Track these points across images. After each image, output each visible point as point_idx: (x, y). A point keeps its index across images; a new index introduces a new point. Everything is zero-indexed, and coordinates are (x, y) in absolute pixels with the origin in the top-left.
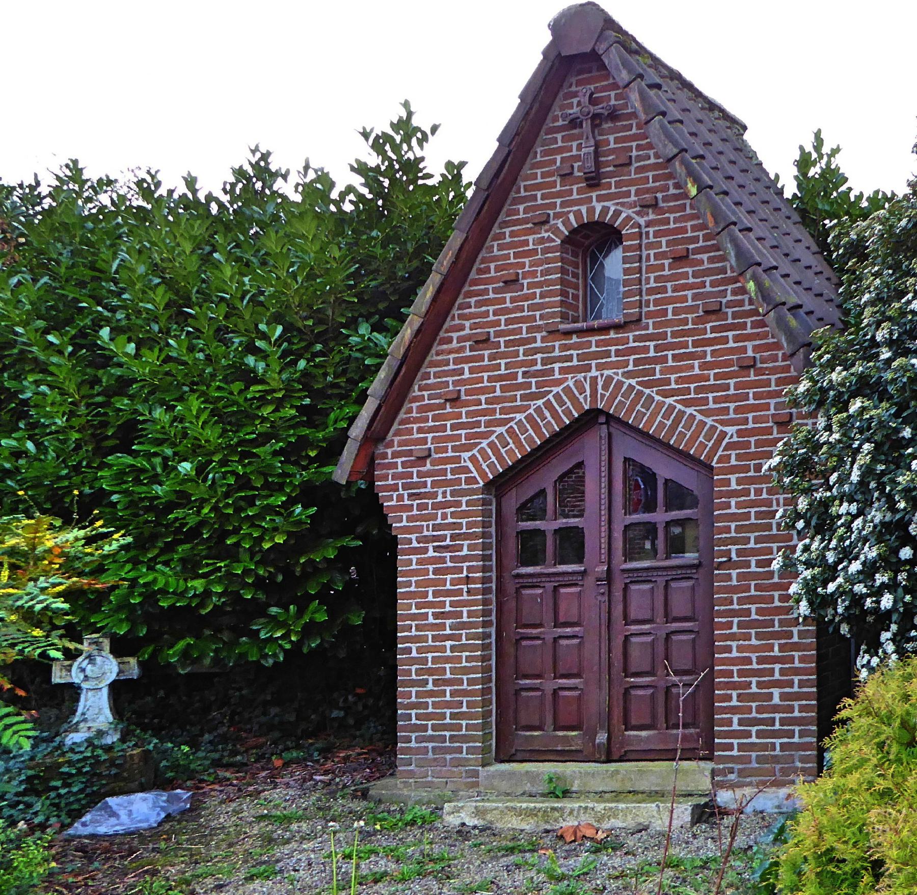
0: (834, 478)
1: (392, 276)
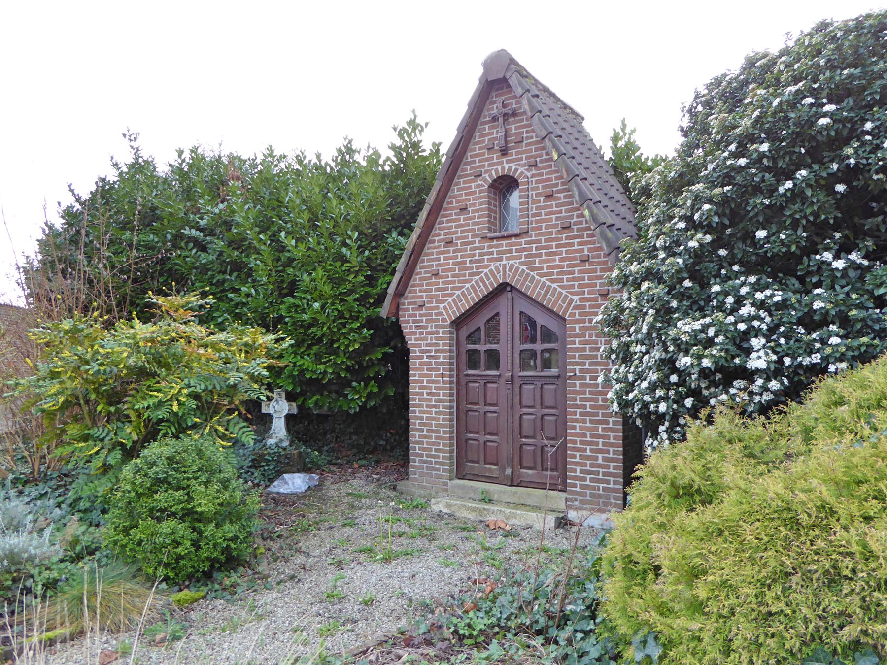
0: (632, 329)
1: (407, 206)
